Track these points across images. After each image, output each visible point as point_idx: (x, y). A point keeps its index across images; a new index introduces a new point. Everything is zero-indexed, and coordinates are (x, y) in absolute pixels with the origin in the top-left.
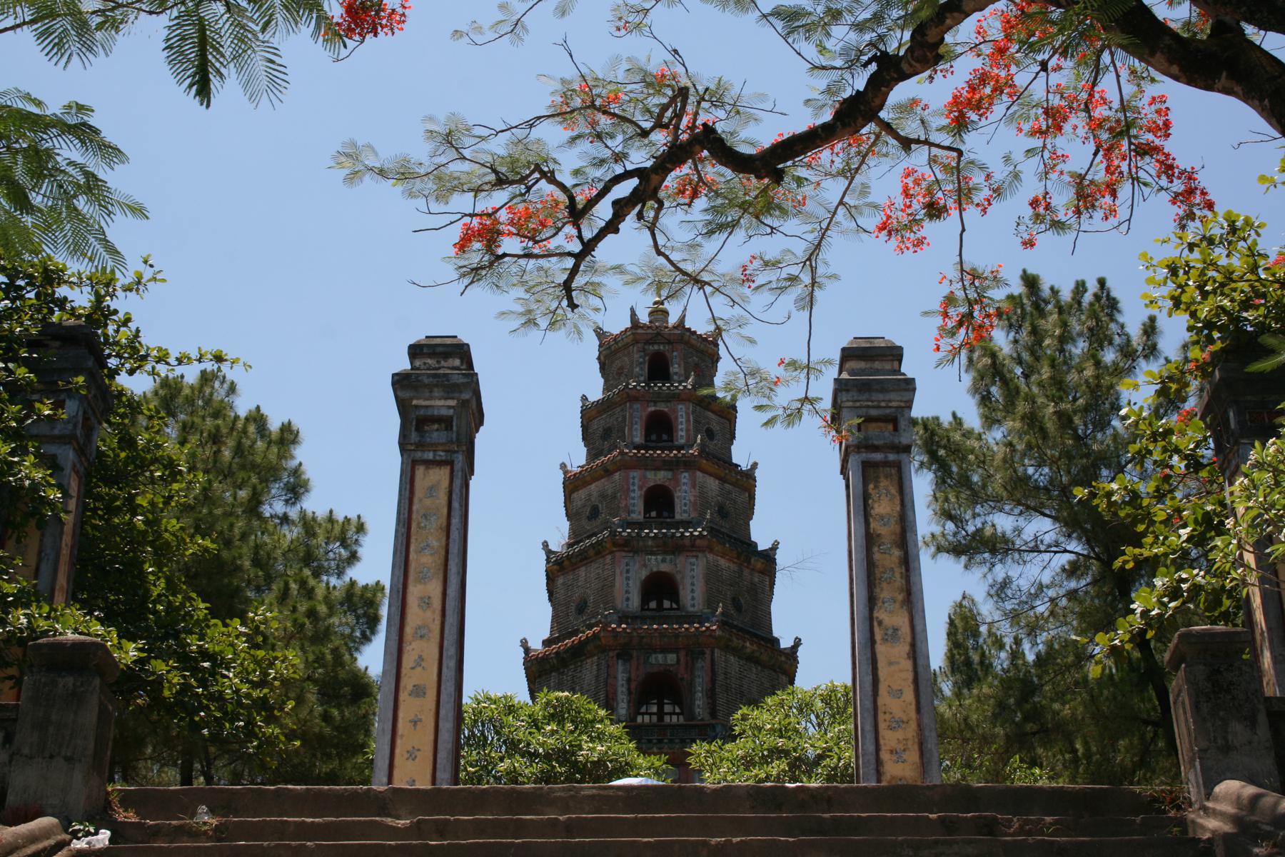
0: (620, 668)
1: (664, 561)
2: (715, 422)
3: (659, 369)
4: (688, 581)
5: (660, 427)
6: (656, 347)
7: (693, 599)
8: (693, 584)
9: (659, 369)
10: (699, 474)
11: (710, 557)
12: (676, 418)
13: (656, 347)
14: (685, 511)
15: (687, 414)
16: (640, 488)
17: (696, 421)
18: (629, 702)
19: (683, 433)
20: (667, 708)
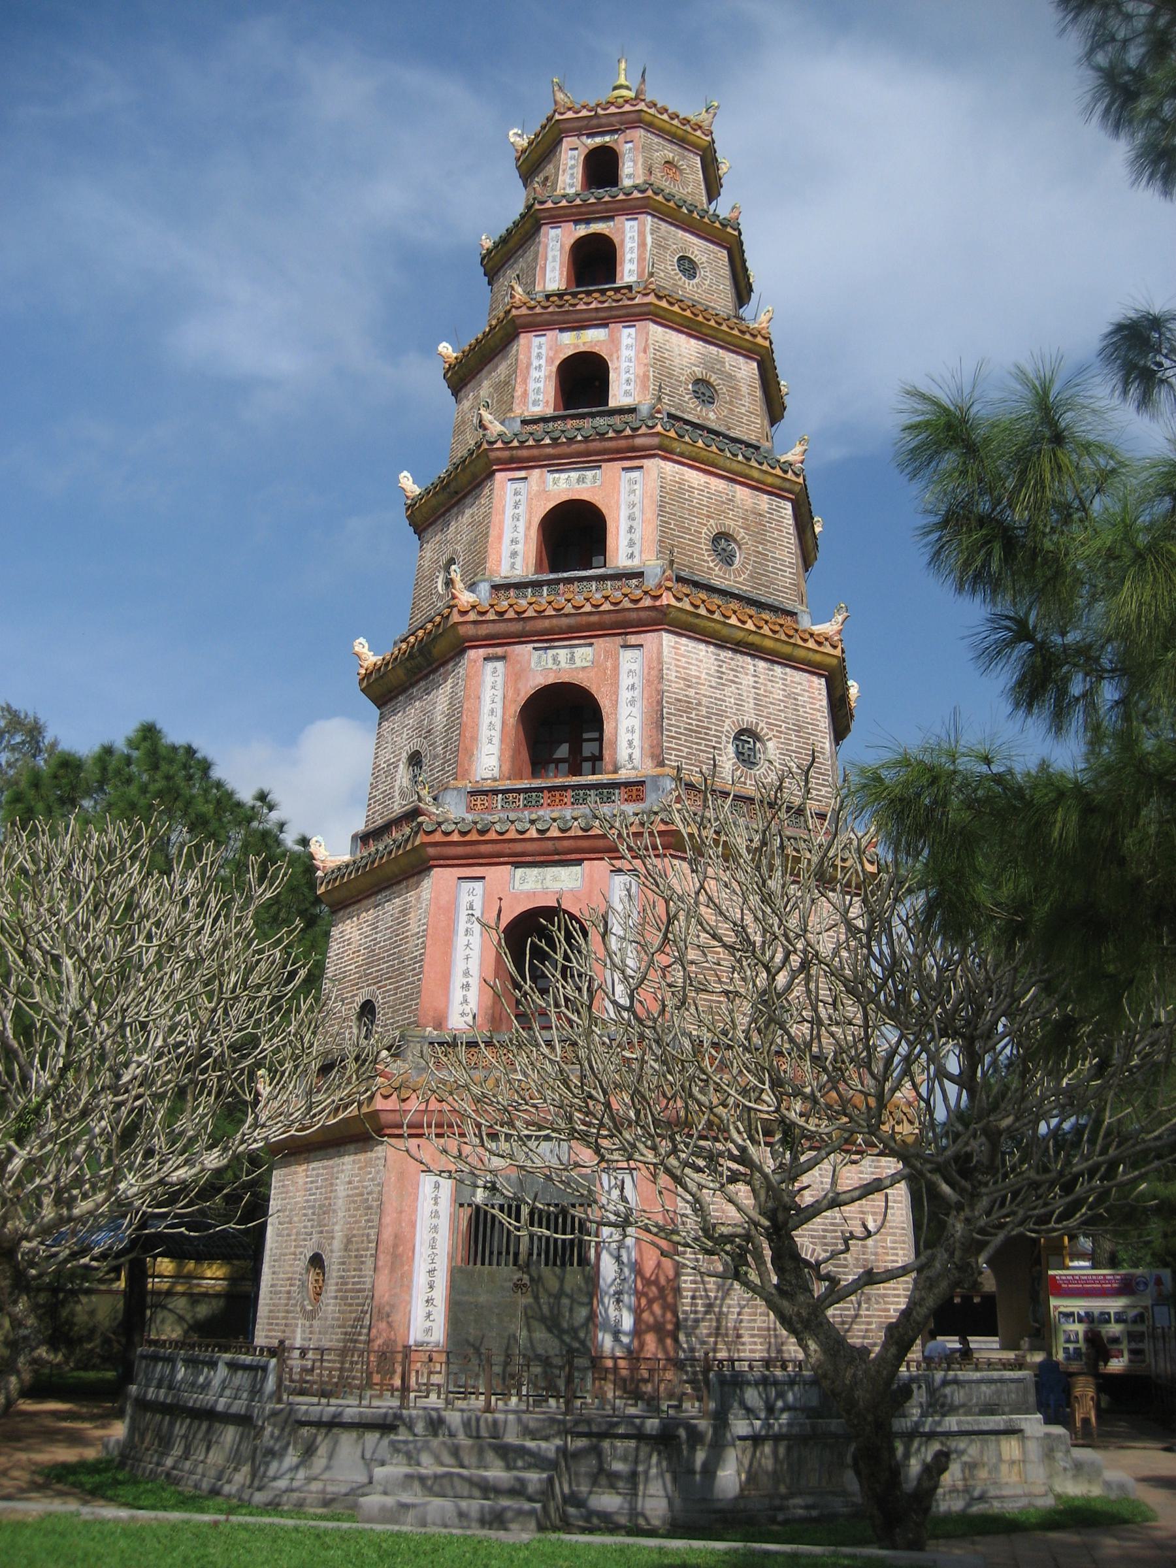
0: (489, 679)
1: (581, 480)
2: (698, 248)
3: (602, 168)
4: (624, 513)
5: (594, 261)
6: (598, 140)
7: (631, 544)
8: (631, 518)
9: (602, 168)
10: (653, 327)
11: (669, 467)
12: (623, 241)
13: (598, 140)
14: (627, 393)
15: (641, 234)
16: (550, 361)
17: (657, 245)
18: (502, 741)
19: (634, 267)
20: (588, 749)
